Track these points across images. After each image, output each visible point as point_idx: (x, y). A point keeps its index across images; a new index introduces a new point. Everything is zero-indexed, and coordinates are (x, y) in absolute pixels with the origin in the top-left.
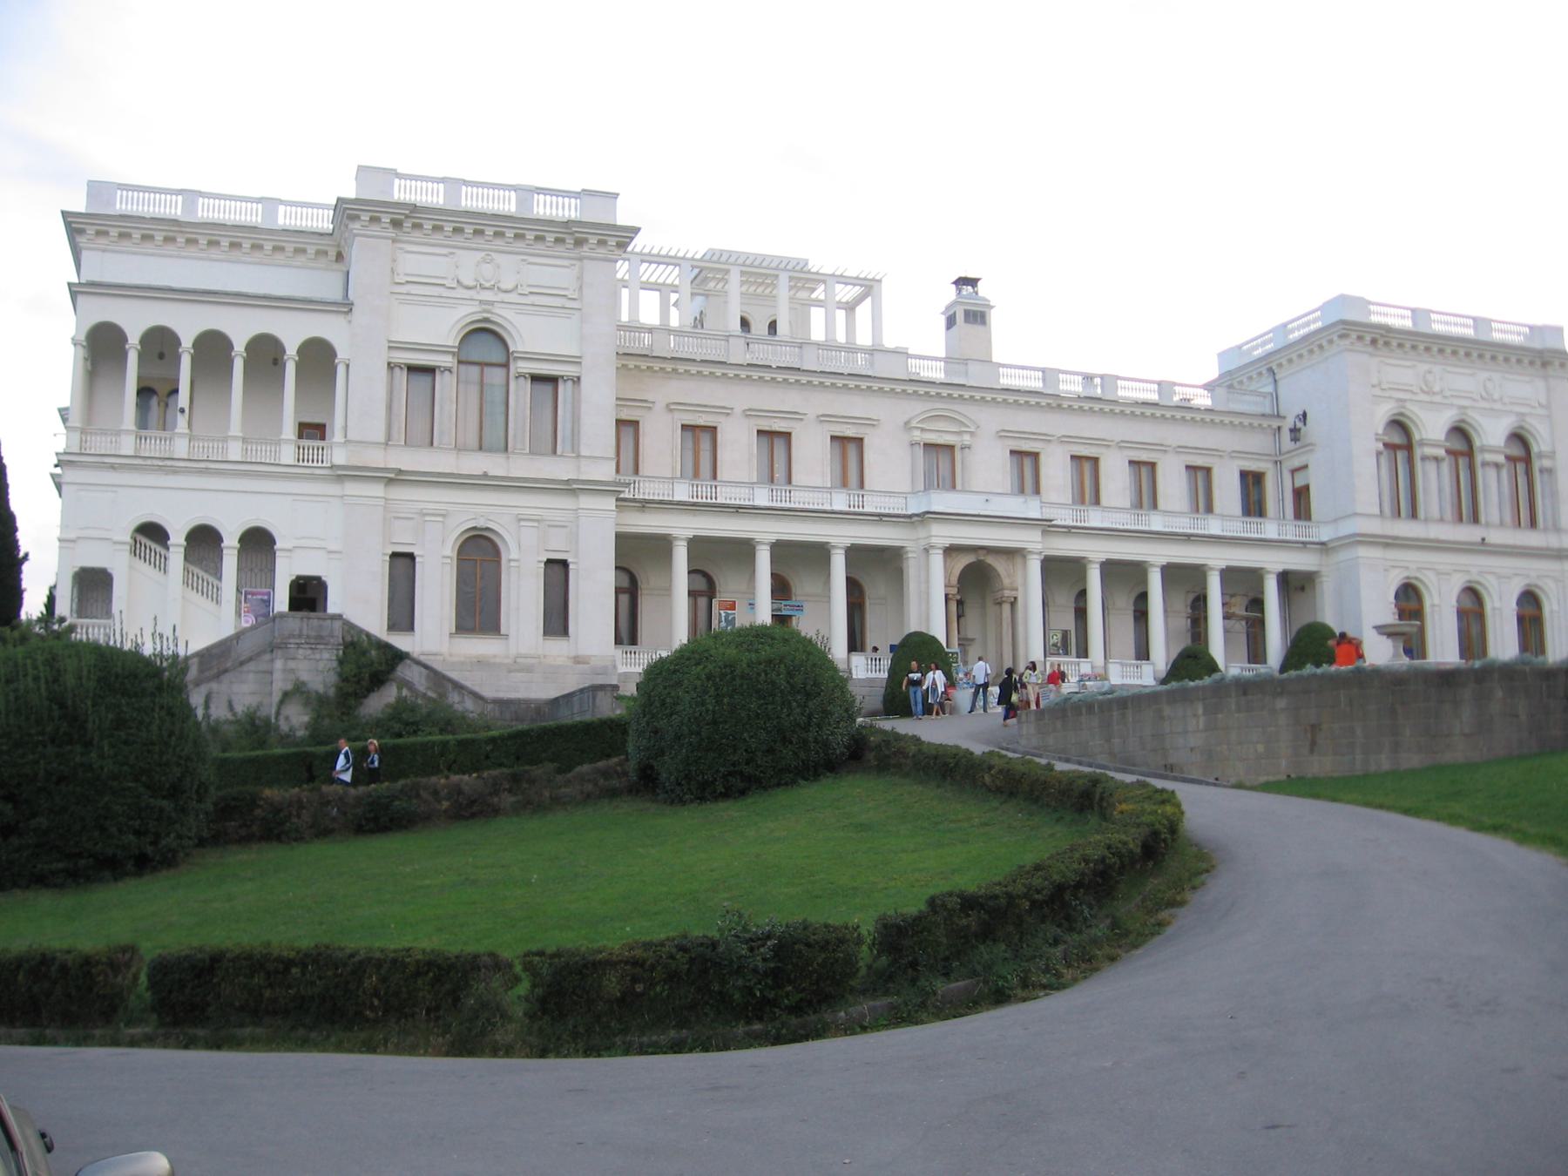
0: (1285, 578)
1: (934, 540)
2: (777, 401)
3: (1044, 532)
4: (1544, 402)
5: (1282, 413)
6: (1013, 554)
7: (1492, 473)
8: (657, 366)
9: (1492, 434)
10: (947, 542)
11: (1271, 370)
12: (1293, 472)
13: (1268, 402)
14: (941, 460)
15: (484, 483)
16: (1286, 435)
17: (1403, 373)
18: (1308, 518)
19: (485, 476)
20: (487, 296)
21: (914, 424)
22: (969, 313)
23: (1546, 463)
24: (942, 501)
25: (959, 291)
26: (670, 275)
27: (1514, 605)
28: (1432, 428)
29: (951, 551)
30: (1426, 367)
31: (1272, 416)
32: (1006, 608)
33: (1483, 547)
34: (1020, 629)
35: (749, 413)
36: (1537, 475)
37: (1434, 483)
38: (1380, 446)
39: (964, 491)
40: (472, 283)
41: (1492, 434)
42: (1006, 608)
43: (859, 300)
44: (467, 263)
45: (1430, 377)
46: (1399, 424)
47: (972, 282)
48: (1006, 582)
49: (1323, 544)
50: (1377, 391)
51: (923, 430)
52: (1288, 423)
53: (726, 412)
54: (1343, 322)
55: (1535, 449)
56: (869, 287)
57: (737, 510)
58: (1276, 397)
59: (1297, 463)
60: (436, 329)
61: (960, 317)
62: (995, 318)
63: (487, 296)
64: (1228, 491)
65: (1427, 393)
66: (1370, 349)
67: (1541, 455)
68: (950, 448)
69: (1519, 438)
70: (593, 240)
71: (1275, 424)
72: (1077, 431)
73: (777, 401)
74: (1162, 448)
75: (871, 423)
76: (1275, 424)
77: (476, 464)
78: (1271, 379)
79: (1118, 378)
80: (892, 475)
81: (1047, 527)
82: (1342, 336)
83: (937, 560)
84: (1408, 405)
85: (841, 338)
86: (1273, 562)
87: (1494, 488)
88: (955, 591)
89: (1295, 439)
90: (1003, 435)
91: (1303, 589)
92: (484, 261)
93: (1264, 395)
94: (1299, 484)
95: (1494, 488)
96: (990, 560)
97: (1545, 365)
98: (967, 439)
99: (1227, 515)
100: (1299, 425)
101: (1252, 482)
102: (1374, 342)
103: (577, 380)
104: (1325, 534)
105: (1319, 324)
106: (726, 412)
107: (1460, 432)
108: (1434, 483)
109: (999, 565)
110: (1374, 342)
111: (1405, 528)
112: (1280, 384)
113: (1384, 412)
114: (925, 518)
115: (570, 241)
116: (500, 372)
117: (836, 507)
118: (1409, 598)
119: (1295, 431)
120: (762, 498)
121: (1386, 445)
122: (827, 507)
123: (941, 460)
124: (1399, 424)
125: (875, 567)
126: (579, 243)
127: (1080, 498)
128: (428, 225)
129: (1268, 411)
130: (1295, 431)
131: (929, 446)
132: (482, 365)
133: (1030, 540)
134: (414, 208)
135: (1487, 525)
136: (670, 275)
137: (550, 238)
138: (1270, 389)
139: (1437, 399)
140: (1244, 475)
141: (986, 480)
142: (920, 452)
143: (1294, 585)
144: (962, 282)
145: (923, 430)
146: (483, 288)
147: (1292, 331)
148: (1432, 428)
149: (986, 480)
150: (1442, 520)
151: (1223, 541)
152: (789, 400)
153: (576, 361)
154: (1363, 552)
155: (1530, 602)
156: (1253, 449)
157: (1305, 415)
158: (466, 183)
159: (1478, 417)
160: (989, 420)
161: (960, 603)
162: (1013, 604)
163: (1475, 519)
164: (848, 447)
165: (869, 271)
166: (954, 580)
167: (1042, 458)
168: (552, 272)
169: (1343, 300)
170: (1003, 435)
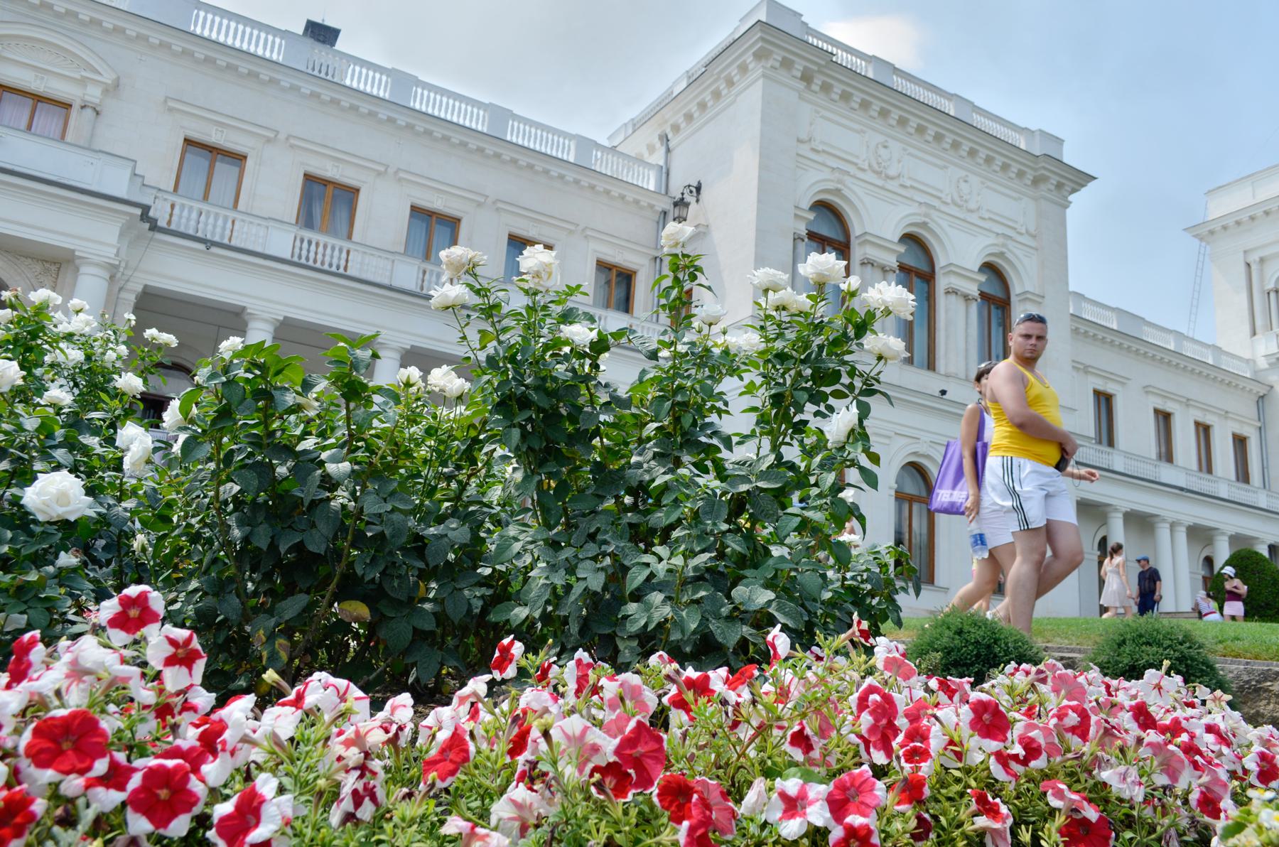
4: (1032, 230)
9: (960, 255)
30: (881, 138)
38: (804, 232)
50: (804, 150)
65: (878, 173)
66: (801, 85)
67: (1025, 296)
78: (663, 149)
84: (848, 180)
100: (688, 198)
102: (807, 78)
157: (698, 189)
159: (944, 224)
163: (931, 365)
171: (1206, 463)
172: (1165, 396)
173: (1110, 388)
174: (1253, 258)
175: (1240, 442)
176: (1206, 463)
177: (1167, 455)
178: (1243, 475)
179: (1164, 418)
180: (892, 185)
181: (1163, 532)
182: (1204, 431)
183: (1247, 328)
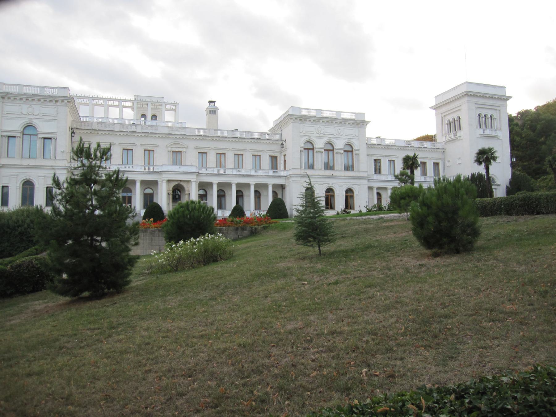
2: (128, 141)
3: (197, 175)
5: (284, 139)
6: (188, 181)
8: (93, 132)
9: (339, 145)
10: (167, 179)
14: (177, 156)
15: (28, 167)
17: (310, 129)
19: (28, 165)
20: (30, 117)
23: (357, 152)
27: (344, 193)
28: (320, 144)
29: (169, 181)
30: (319, 126)
35: (120, 144)
36: (354, 156)
38: (302, 149)
40: (26, 113)
41: (339, 145)
44: (25, 108)
47: (214, 102)
60: (15, 126)
62: (219, 112)
63: (30, 117)
64: (266, 162)
70: (60, 101)
73: (128, 141)
74: (245, 150)
75: (157, 146)
77: (26, 162)
82: (291, 119)
90: (196, 148)
92: (29, 107)
96: (182, 183)
98: (184, 150)
101: (274, 159)
102: (300, 120)
103: (56, 139)
113: (305, 139)
115: (54, 101)
116: (35, 136)
123: (177, 156)
126: (57, 101)
128: (12, 98)
132: (30, 135)
133: (193, 178)
134: (7, 94)
137: (48, 100)
139: (321, 135)
141: (191, 161)
144: (210, 102)
146: (29, 114)
148: (320, 144)
149: (191, 161)
150: (321, 169)
152: (132, 140)
153: (55, 134)
154: (293, 179)
156: (275, 149)
158: (24, 86)
159: (334, 140)
160: (192, 144)
164: (149, 152)
166: (171, 189)
168: (49, 109)
170: (196, 148)
175: (436, 165)
180: (321, 135)
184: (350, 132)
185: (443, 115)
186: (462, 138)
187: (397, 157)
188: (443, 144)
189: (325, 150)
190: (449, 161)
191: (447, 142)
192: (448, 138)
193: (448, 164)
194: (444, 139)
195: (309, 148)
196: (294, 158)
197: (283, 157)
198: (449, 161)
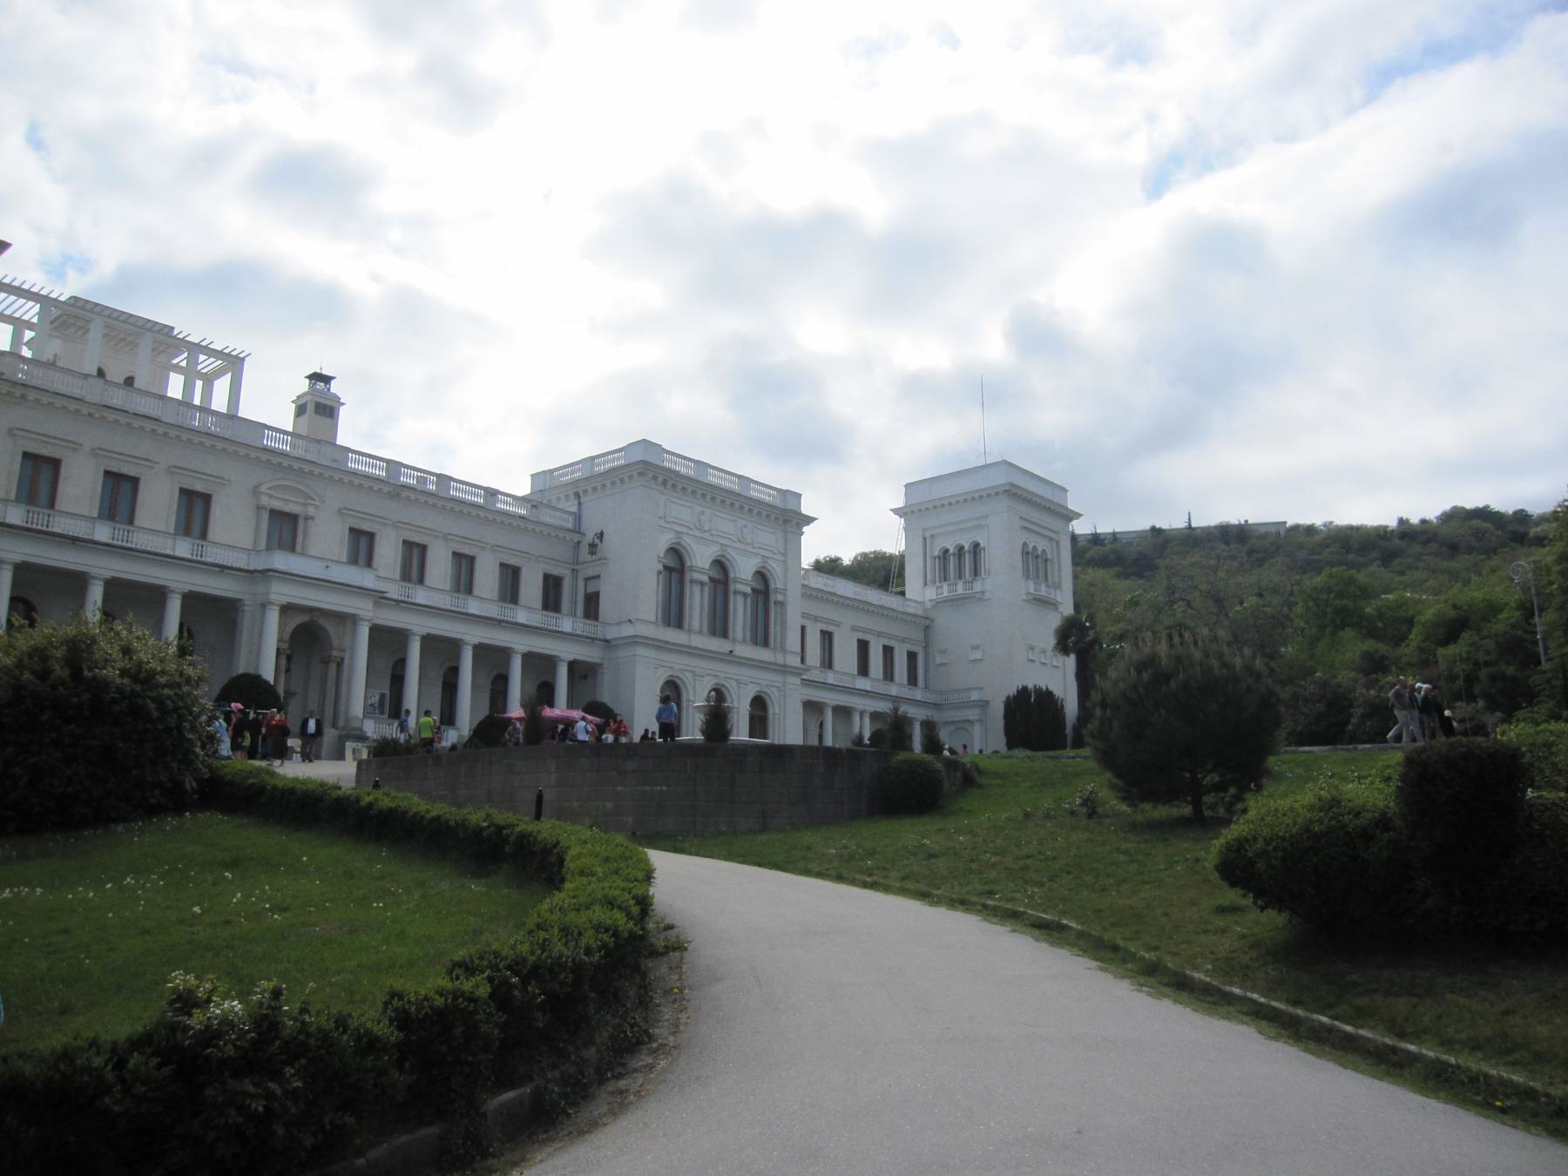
0: (572, 665)
1: (273, 597)
3: (376, 604)
6: (347, 620)
7: (740, 600)
9: (744, 570)
10: (284, 600)
11: (577, 495)
12: (587, 580)
13: (571, 519)
16: (584, 549)
17: (684, 511)
18: (596, 618)
21: (263, 488)
22: (320, 404)
23: (780, 598)
24: (282, 561)
25: (312, 386)
26: (30, 312)
29: (287, 609)
31: (573, 531)
32: (333, 667)
33: (729, 658)
34: (344, 687)
36: (772, 606)
37: (697, 603)
38: (661, 567)
39: (302, 554)
42: (333, 667)
43: (218, 373)
45: (703, 518)
46: (676, 552)
47: (326, 379)
48: (335, 643)
49: (607, 641)
51: (271, 496)
52: (589, 537)
53: (75, 447)
54: (644, 462)
55: (772, 586)
56: (233, 363)
57: (74, 541)
58: (578, 517)
59: (590, 573)
61: (310, 408)
62: (344, 414)
64: (532, 588)
68: (294, 518)
69: (761, 575)
71: (576, 538)
72: (416, 517)
76: (576, 538)
79: (451, 479)
80: (234, 531)
81: (380, 598)
82: (640, 474)
83: (273, 617)
85: (197, 401)
86: (566, 652)
87: (740, 613)
88: (285, 646)
89: (592, 553)
91: (585, 677)
93: (570, 513)
94: (590, 590)
95: (740, 613)
96: (322, 621)
97: (786, 522)
99: (528, 610)
102: (664, 483)
104: (612, 633)
105: (622, 462)
106: (75, 447)
107: (720, 564)
108: (697, 603)
109: (331, 628)
110: (664, 483)
111: (672, 635)
112: (585, 507)
113: (665, 541)
114: (266, 574)
117: (178, 553)
118: (672, 692)
119: (593, 546)
120: (103, 533)
121: (665, 567)
122: (169, 552)
123: (285, 528)
124: (676, 552)
125: (213, 617)
127: (406, 576)
129: (570, 526)
130: (593, 546)
131: (274, 513)
133: (364, 609)
135: (734, 640)
136: (30, 312)
138: (574, 509)
140: (547, 577)
142: (265, 516)
143: (581, 673)
144: (316, 377)
145: (271, 496)
147: (599, 465)
148: (701, 558)
150: (701, 632)
151: (527, 631)
154: (640, 651)
155: (759, 704)
157: (602, 534)
161: (289, 658)
162: (340, 664)
165: (235, 345)
166: (287, 636)
167: (378, 538)
169: (645, 443)
171: (889, 675)
172: (863, 630)
173: (830, 628)
174: (928, 534)
175: (912, 656)
176: (889, 675)
177: (863, 670)
178: (912, 680)
179: (863, 647)
180: (707, 536)
181: (857, 718)
182: (888, 651)
183: (921, 581)
184: (768, 538)
185: (928, 534)
186: (987, 596)
187: (838, 625)
188: (929, 605)
189: (711, 579)
190: (943, 652)
191: (938, 604)
192: (946, 591)
193: (939, 659)
194: (930, 594)
195: (675, 567)
196: (633, 592)
197: (581, 584)
198: (943, 652)
